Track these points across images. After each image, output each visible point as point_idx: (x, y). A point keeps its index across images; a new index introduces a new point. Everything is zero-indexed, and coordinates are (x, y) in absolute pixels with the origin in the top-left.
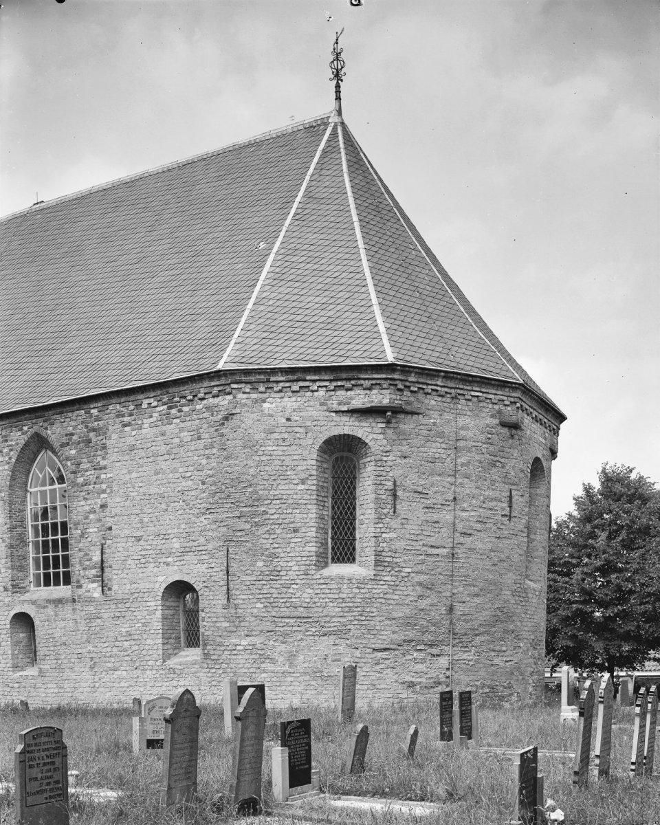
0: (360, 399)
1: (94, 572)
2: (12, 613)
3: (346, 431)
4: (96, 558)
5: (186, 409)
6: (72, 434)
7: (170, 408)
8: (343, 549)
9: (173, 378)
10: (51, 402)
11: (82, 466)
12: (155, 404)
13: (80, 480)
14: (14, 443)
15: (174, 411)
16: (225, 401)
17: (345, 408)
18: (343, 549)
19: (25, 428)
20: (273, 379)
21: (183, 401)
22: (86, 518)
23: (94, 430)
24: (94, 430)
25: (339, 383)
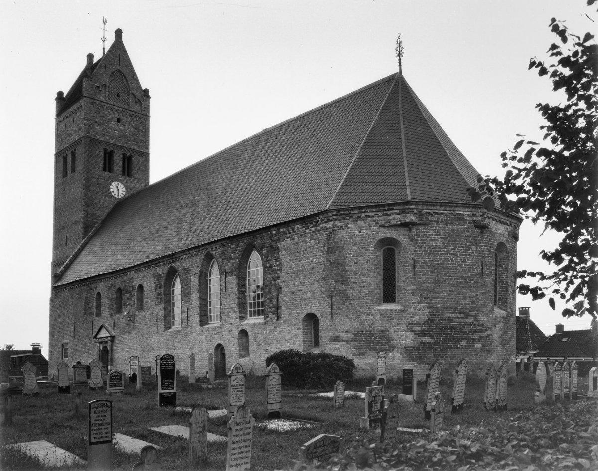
0: (395, 218)
1: (273, 309)
2: (240, 329)
3: (389, 235)
4: (274, 302)
5: (313, 229)
6: (265, 243)
7: (306, 229)
8: (389, 295)
9: (307, 215)
10: (256, 229)
11: (269, 258)
12: (300, 227)
13: (268, 265)
14: (240, 248)
15: (308, 230)
16: (330, 225)
17: (387, 224)
18: (389, 295)
19: (245, 241)
20: (352, 212)
21: (312, 225)
22: (271, 283)
23: (274, 241)
24: (274, 241)
25: (385, 212)
